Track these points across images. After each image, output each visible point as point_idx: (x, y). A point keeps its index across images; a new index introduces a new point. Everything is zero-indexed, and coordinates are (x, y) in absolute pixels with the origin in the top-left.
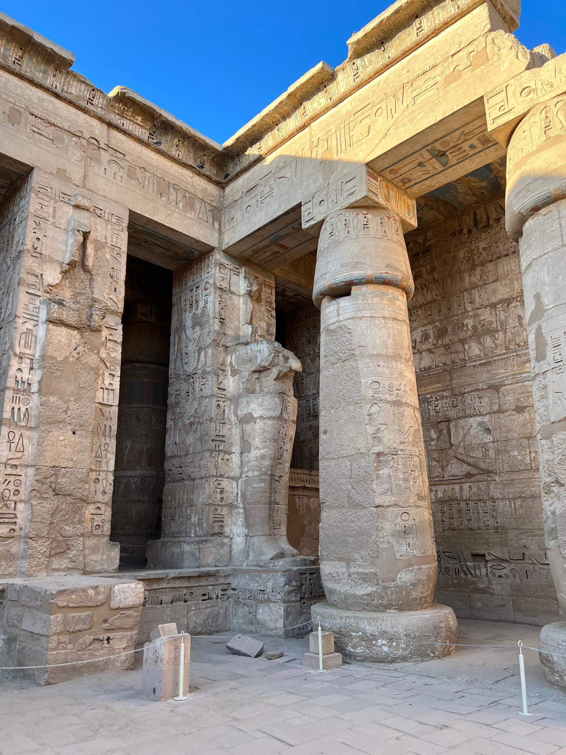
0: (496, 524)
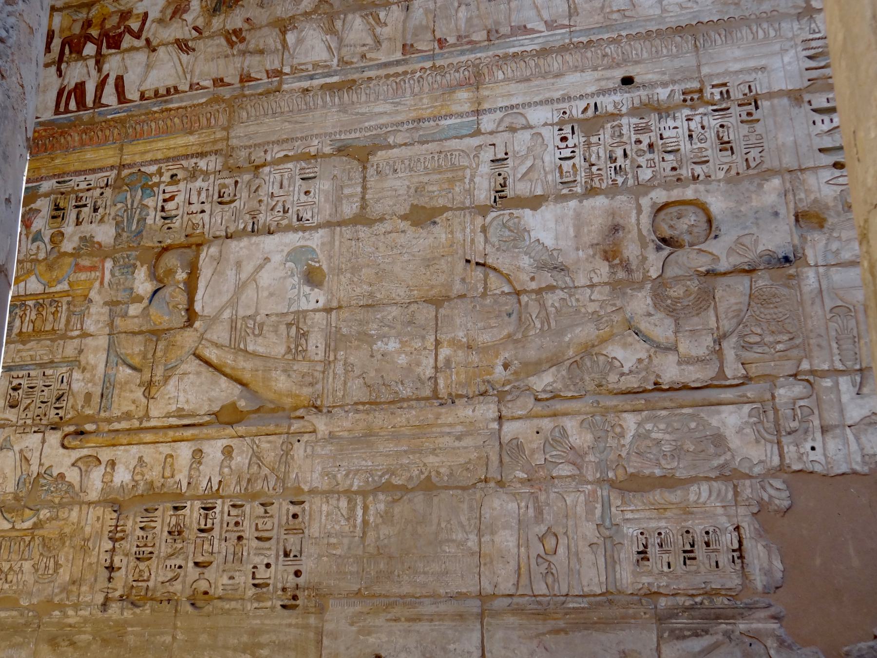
0: (291, 577)
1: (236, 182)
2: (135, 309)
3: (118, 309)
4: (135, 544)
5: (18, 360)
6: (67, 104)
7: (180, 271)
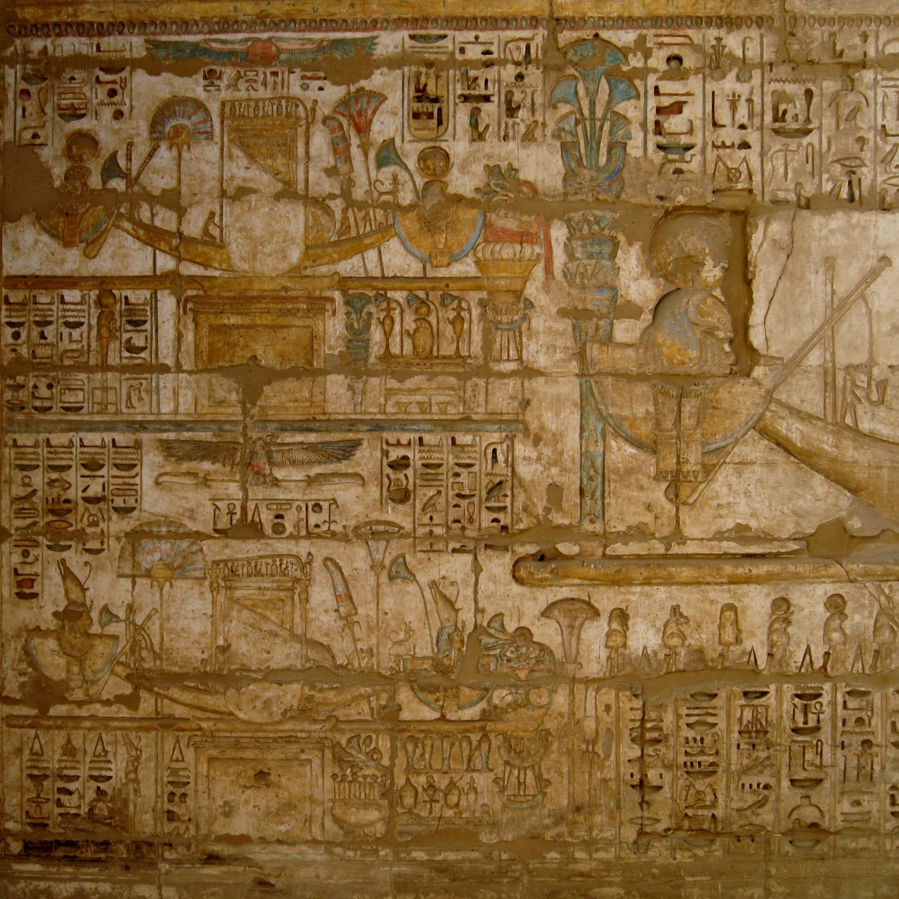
1: (809, 94)
2: (627, 330)
3: (590, 326)
4: (683, 750)
5: (393, 410)
7: (709, 263)
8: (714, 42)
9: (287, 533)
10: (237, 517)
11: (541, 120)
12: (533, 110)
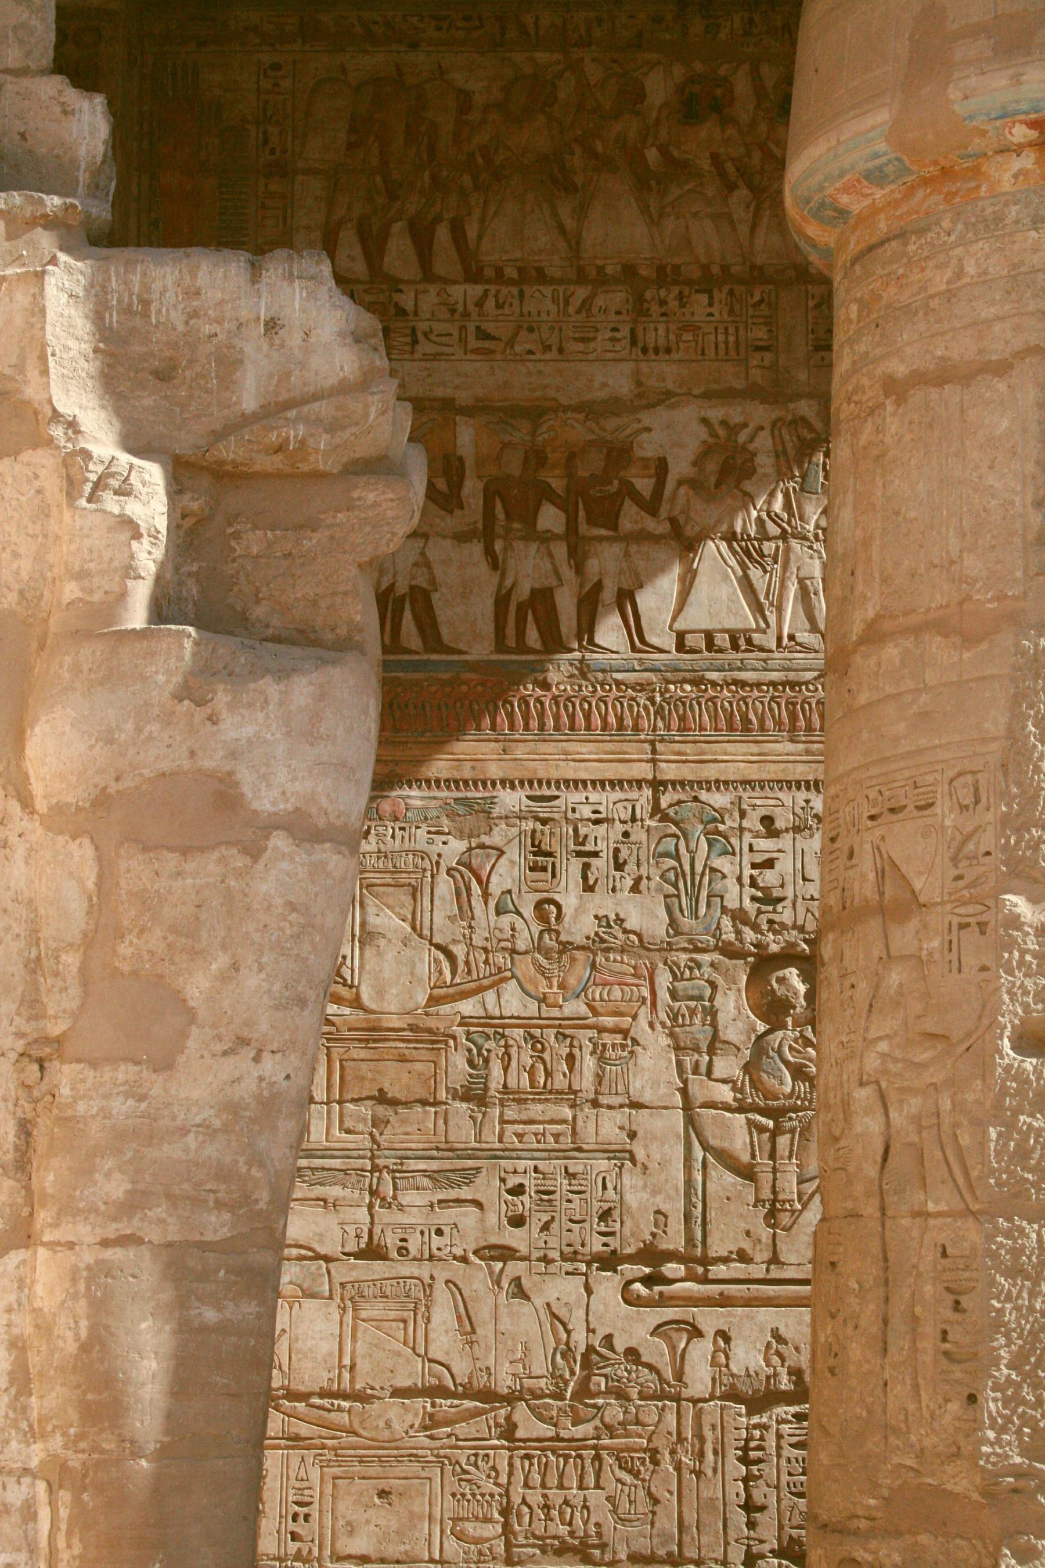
6: (521, 634)
8: (804, 804)
9: (411, 1256)
10: (365, 1239)
11: (645, 875)
12: (638, 865)
